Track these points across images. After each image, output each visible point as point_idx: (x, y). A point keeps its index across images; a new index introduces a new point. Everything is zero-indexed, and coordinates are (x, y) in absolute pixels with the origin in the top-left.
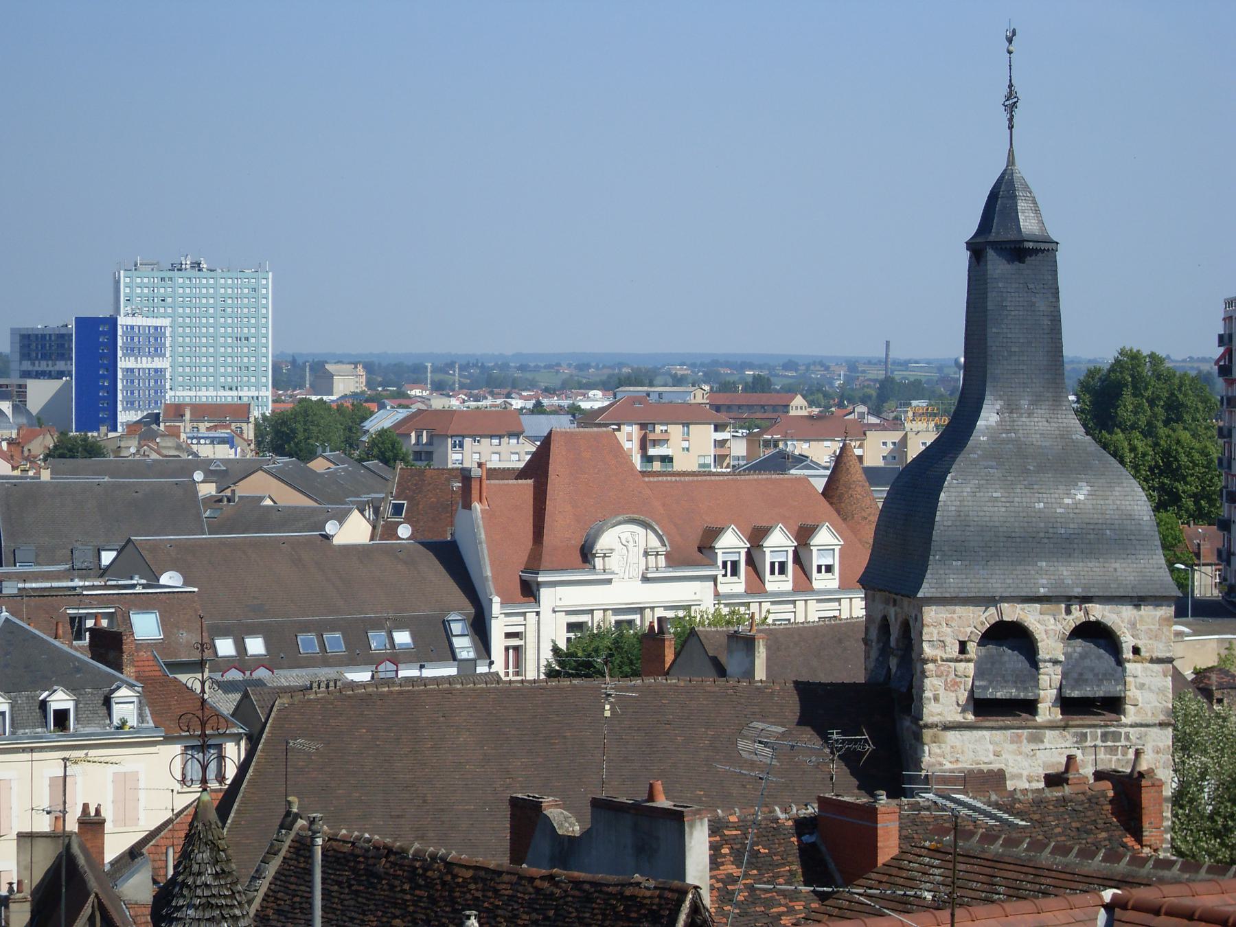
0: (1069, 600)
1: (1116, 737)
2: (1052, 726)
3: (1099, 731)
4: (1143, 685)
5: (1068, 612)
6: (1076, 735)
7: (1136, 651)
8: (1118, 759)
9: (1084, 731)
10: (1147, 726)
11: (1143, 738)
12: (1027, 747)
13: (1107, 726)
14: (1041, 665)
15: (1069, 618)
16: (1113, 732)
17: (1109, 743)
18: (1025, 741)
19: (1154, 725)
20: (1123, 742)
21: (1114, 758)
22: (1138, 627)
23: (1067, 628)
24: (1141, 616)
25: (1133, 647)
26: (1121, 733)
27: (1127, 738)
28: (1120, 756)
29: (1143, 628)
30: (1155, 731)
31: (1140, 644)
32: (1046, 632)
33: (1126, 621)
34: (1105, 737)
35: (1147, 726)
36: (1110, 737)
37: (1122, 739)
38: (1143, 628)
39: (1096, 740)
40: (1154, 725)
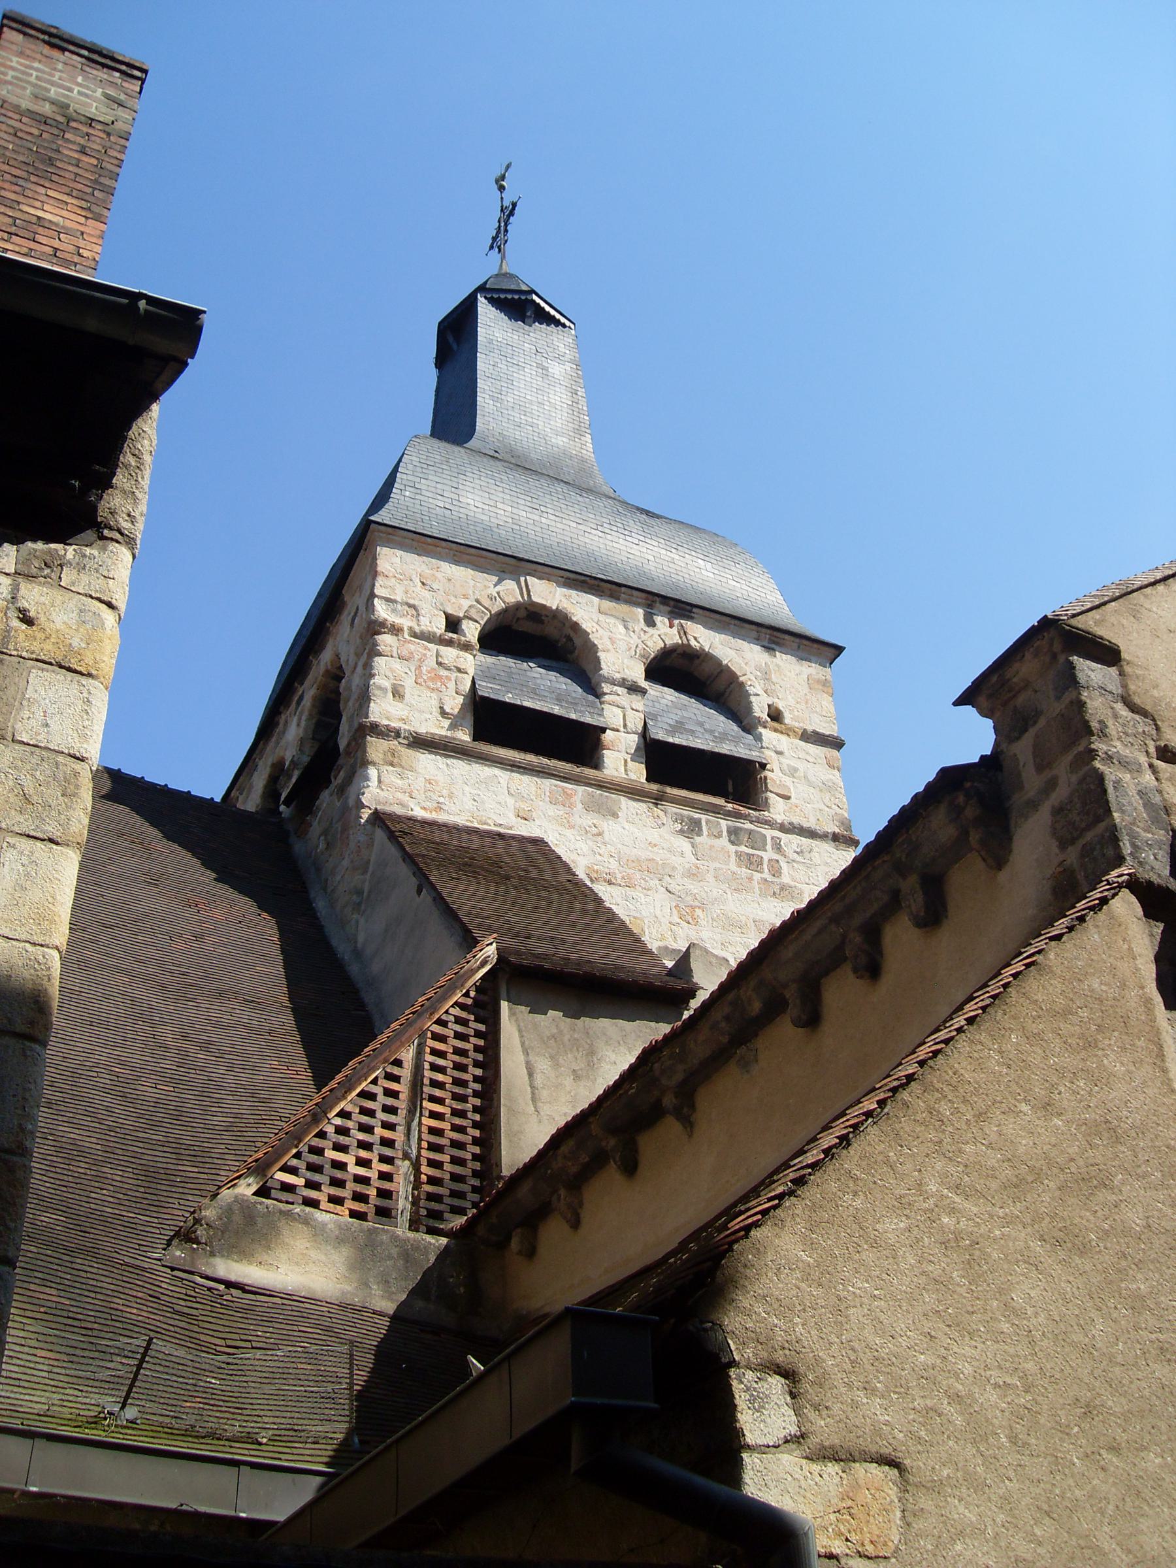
2: (633, 792)
3: (724, 824)
5: (650, 623)
6: (679, 819)
7: (776, 716)
9: (696, 816)
13: (737, 815)
16: (750, 832)
17: (743, 848)
18: (580, 806)
19: (823, 836)
21: (757, 876)
27: (778, 847)
28: (766, 875)
30: (827, 847)
31: (781, 705)
37: (769, 847)
40: (823, 836)
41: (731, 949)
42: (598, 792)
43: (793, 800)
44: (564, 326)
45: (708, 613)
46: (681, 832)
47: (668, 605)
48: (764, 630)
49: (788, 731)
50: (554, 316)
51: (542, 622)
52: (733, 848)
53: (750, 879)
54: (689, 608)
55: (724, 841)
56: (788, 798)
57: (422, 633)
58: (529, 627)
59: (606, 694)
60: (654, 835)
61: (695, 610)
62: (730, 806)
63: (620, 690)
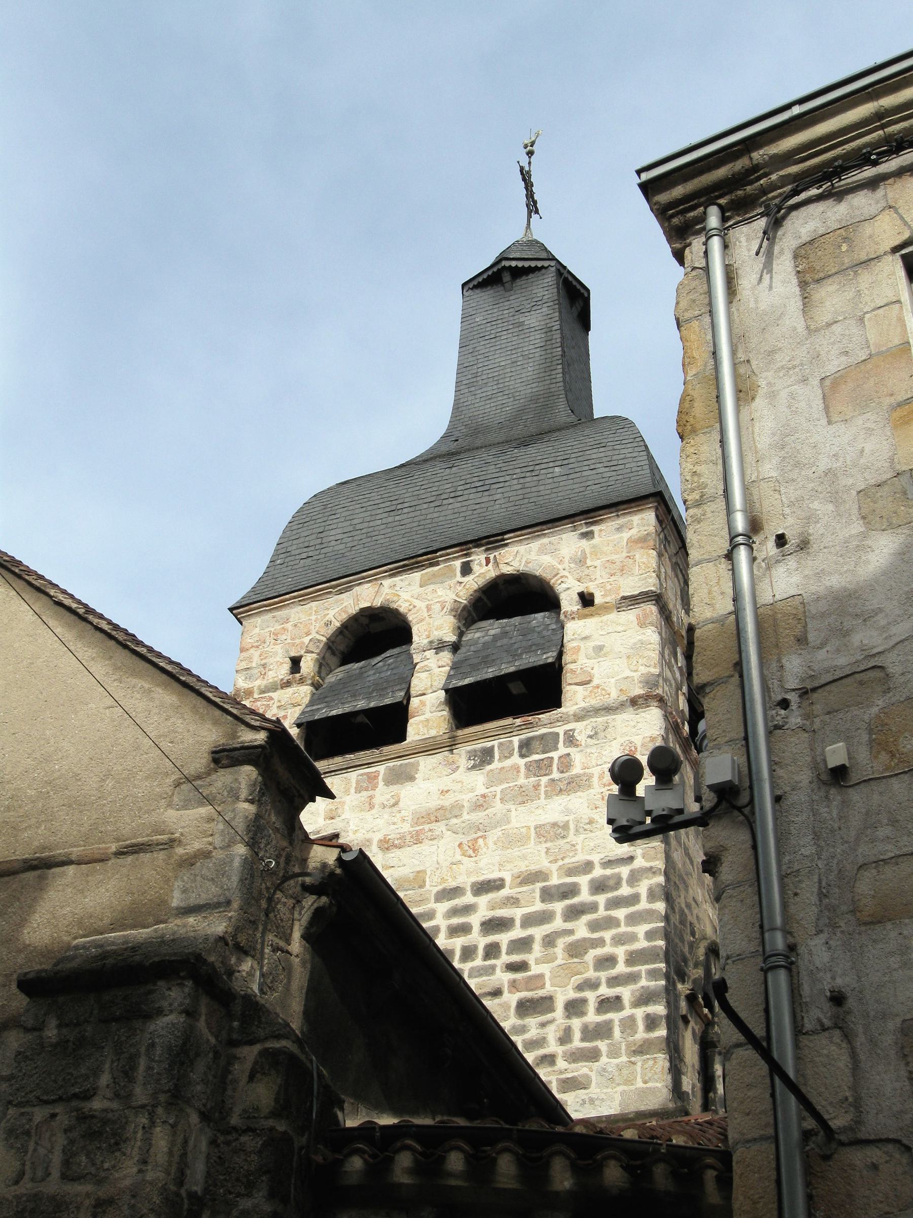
0: (466, 545)
1: (549, 743)
2: (429, 748)
4: (600, 648)
5: (466, 570)
6: (472, 755)
7: (586, 600)
8: (553, 780)
9: (489, 744)
10: (608, 709)
11: (602, 734)
12: (382, 793)
13: (529, 726)
14: (416, 658)
15: (469, 579)
16: (542, 737)
18: (381, 783)
20: (562, 750)
21: (544, 780)
22: (589, 563)
23: (461, 594)
24: (594, 546)
25: (582, 595)
26: (557, 734)
27: (571, 740)
28: (556, 775)
29: (597, 563)
30: (627, 717)
31: (591, 587)
32: (429, 608)
33: (566, 560)
34: (526, 747)
35: (608, 709)
36: (536, 744)
38: (597, 563)
39: (511, 755)
41: (509, 866)
42: (399, 763)
43: (595, 682)
44: (543, 267)
45: (519, 533)
46: (473, 767)
47: (482, 545)
48: (577, 518)
49: (606, 608)
50: (536, 267)
51: (383, 619)
52: (522, 762)
53: (536, 787)
54: (499, 538)
55: (516, 759)
56: (589, 682)
57: (266, 687)
58: (377, 627)
59: (417, 664)
60: (446, 782)
61: (506, 537)
62: (518, 721)
63: (428, 654)
